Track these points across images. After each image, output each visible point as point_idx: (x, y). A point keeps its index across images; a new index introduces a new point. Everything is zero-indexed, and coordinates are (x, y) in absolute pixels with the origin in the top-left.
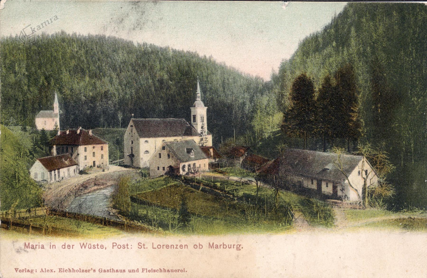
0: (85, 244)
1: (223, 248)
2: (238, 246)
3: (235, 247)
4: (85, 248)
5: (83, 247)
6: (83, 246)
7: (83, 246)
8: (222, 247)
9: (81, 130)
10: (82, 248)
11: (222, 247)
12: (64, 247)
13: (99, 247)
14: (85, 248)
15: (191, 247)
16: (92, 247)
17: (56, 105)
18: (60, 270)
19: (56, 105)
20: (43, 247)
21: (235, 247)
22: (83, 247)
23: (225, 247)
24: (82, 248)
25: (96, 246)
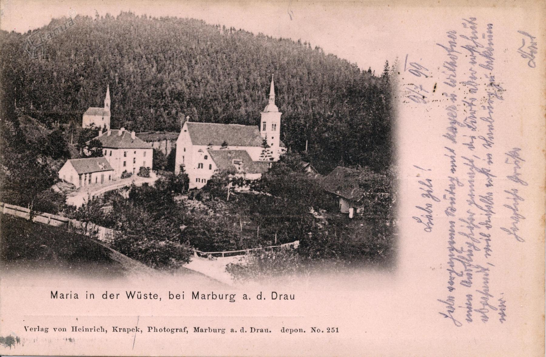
0: (133, 293)
1: (213, 298)
2: (232, 297)
3: (228, 297)
4: (133, 297)
5: (131, 297)
6: (131, 296)
7: (131, 296)
8: (210, 297)
9: (123, 132)
10: (128, 297)
11: (210, 297)
12: (105, 296)
13: (152, 297)
14: (133, 297)
15: (123, 296)
16: (143, 297)
17: (108, 101)
18: (196, 330)
19: (108, 101)
20: (76, 297)
21: (228, 297)
22: (131, 297)
23: (214, 297)
24: (128, 297)
25: (148, 296)
